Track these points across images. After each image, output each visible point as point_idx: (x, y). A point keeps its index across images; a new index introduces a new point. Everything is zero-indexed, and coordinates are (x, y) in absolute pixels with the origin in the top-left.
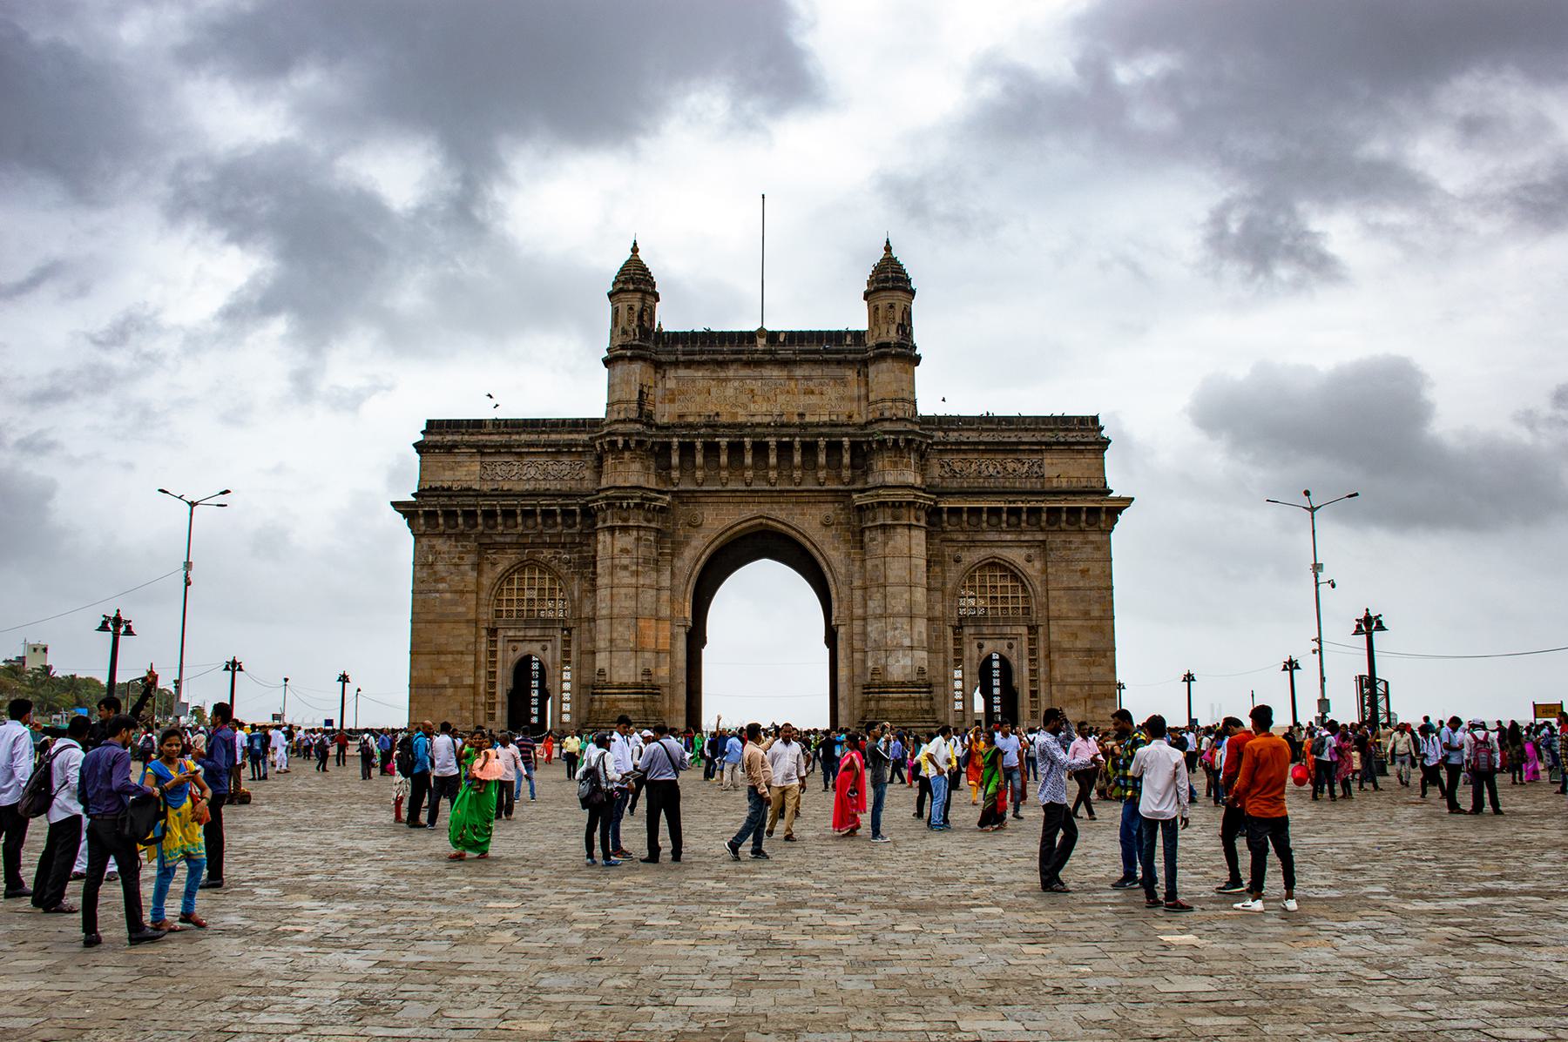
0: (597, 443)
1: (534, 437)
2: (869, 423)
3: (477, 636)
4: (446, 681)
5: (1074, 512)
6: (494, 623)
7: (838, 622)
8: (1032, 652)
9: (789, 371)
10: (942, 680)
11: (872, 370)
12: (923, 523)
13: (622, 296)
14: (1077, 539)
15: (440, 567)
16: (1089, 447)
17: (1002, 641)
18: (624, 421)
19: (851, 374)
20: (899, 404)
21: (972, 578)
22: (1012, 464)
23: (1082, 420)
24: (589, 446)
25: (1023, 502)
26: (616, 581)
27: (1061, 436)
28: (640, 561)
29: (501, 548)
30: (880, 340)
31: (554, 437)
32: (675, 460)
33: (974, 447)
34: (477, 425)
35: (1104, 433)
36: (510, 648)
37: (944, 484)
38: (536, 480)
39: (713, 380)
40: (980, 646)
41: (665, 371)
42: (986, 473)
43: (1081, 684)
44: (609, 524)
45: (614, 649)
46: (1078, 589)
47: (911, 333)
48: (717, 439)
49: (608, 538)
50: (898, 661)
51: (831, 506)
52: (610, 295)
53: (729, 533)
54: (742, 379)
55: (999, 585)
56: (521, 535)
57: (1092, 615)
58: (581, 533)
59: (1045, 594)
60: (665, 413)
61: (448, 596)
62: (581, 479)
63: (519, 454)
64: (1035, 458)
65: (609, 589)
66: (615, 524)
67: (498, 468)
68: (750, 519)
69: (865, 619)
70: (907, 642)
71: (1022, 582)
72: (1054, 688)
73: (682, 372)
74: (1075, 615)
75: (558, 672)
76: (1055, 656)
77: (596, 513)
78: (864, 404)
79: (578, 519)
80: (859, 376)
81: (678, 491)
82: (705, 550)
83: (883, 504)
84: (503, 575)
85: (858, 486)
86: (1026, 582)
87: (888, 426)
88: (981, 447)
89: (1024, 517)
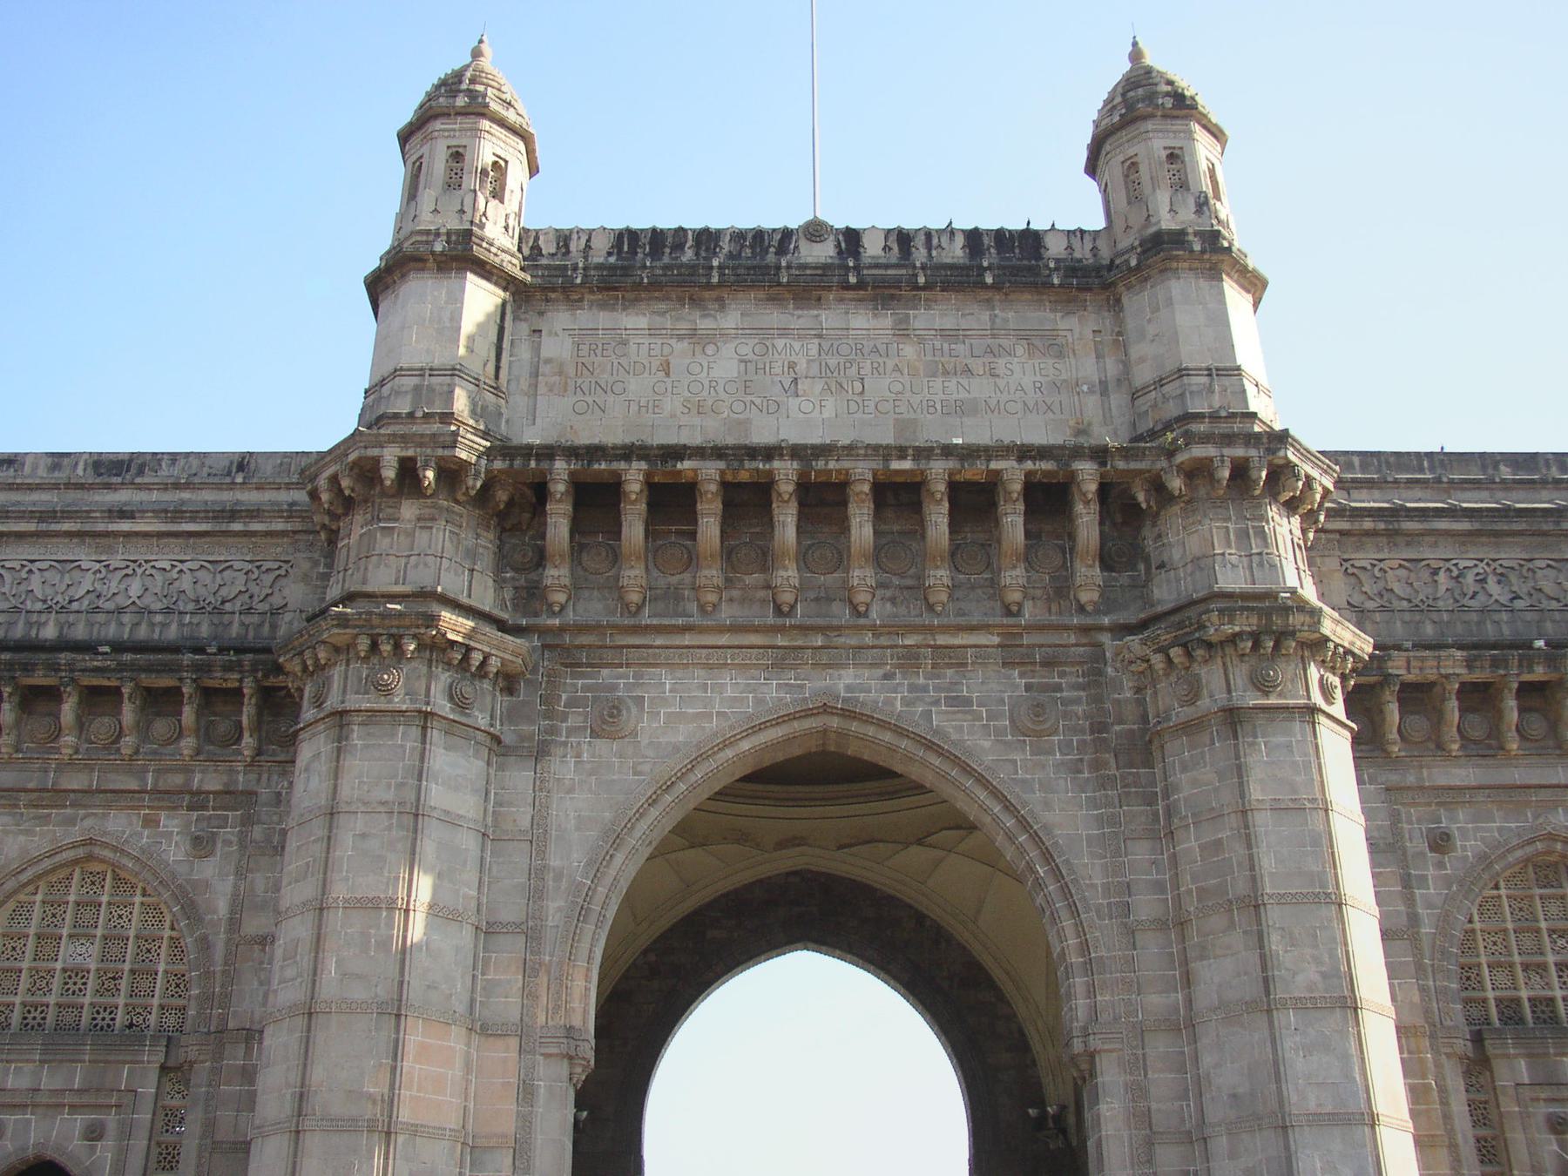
7: (1095, 1043)
11: (1136, 302)
13: (438, 125)
30: (1152, 230)
39: (680, 338)
44: (333, 702)
45: (308, 1124)
52: (405, 137)
54: (763, 333)
62: (276, 612)
65: (310, 917)
66: (348, 706)
67: (35, 583)
68: (792, 717)
69: (1185, 1025)
77: (301, 690)
78: (1118, 400)
81: (562, 629)
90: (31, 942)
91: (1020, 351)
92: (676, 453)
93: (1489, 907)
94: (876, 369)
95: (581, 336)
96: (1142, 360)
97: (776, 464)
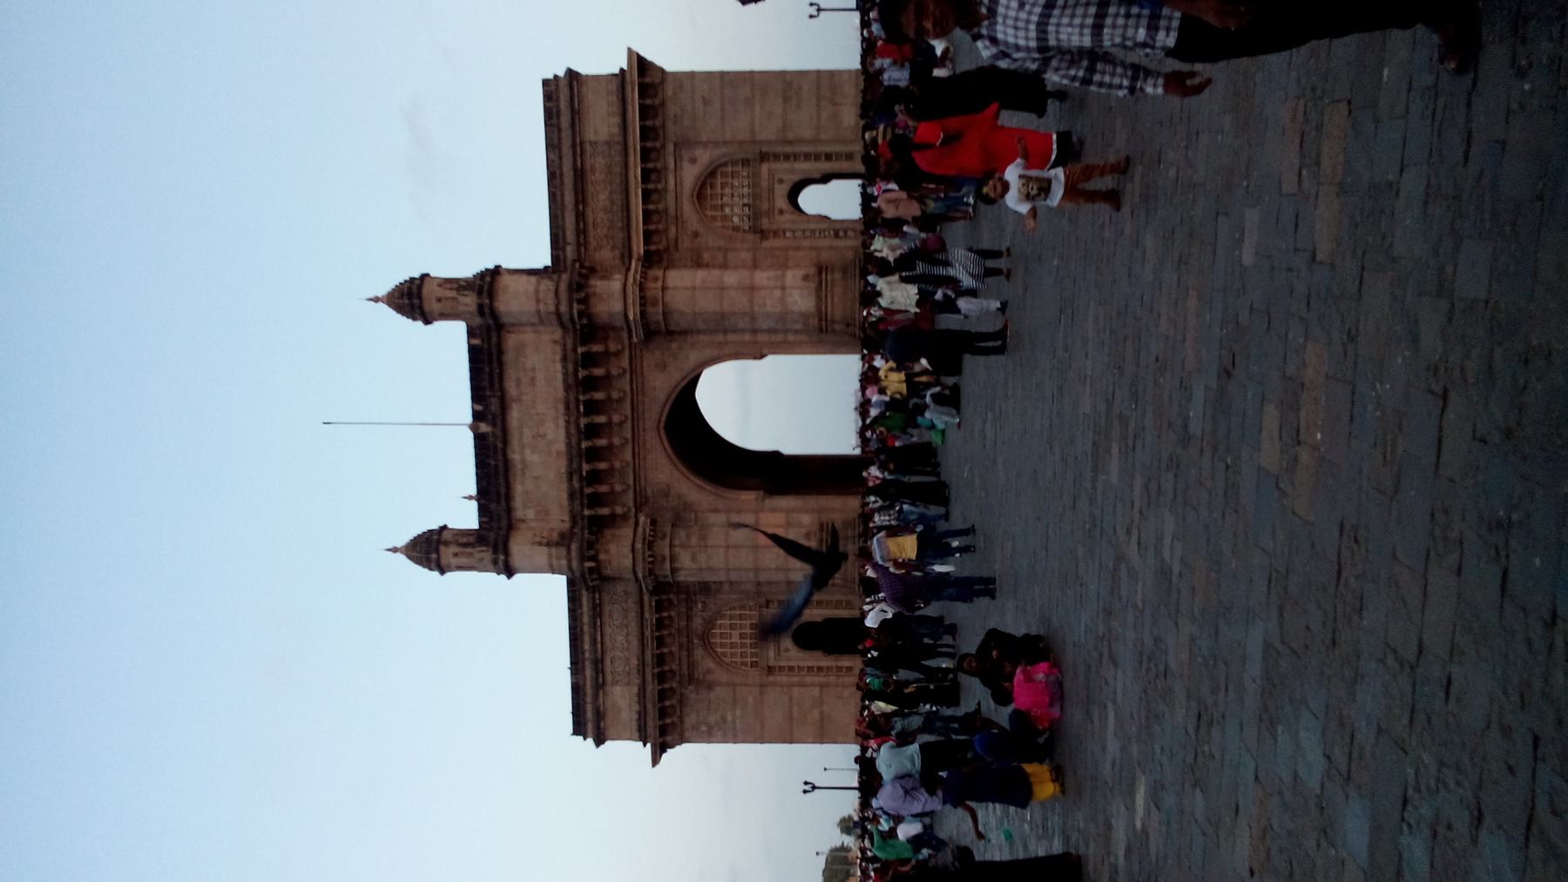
0: (591, 584)
1: (587, 639)
2: (562, 324)
3: (774, 684)
4: (816, 712)
5: (645, 112)
6: (763, 669)
8: (787, 157)
9: (513, 400)
10: (814, 254)
11: (505, 320)
12: (660, 273)
14: (672, 109)
15: (712, 719)
16: (576, 93)
17: (775, 191)
18: (569, 560)
19: (511, 341)
20: (542, 295)
21: (714, 218)
22: (597, 175)
23: (548, 97)
24: (593, 590)
25: (636, 167)
26: (722, 566)
27: (565, 121)
28: (703, 543)
29: (692, 665)
30: (476, 314)
31: (586, 619)
32: (605, 511)
33: (580, 216)
34: (577, 690)
35: (561, 73)
36: (786, 654)
37: (620, 246)
38: (628, 634)
39: (524, 474)
40: (781, 212)
41: (518, 520)
42: (607, 202)
43: (818, 106)
44: (669, 573)
46: (722, 110)
47: (466, 280)
48: (584, 474)
49: (682, 573)
50: (796, 302)
51: (645, 364)
52: (442, 572)
53: (674, 457)
54: (523, 447)
55: (719, 191)
56: (681, 646)
58: (678, 594)
60: (559, 518)
61: (738, 712)
63: (603, 653)
64: (588, 147)
66: (669, 568)
67: (618, 669)
68: (660, 438)
70: (778, 293)
71: (717, 168)
72: (823, 137)
73: (518, 502)
76: (791, 136)
78: (541, 328)
79: (664, 597)
80: (513, 332)
82: (691, 481)
83: (643, 314)
84: (718, 663)
85: (625, 335)
86: (717, 163)
87: (563, 308)
88: (581, 207)
89: (651, 165)
90: (732, 650)
91: (523, 360)
92: (581, 478)
93: (714, 218)
95: (525, 507)
97: (583, 446)
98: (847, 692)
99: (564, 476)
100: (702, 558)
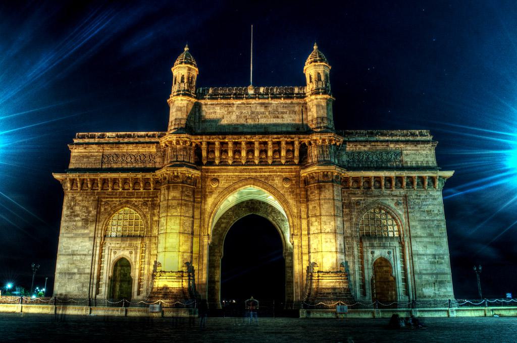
4: (76, 271)
9: (266, 107)
14: (423, 195)
15: (77, 208)
17: (385, 250)
37: (349, 165)
40: (372, 253)
42: (371, 159)
43: (432, 274)
46: (426, 221)
57: (435, 235)
59: (407, 224)
61: (80, 224)
62: (155, 163)
72: (416, 277)
74: (426, 235)
75: (137, 266)
76: (415, 259)
94: (262, 118)
96: (310, 115)
98: (86, 290)
99: (224, 131)
100: (174, 203)
